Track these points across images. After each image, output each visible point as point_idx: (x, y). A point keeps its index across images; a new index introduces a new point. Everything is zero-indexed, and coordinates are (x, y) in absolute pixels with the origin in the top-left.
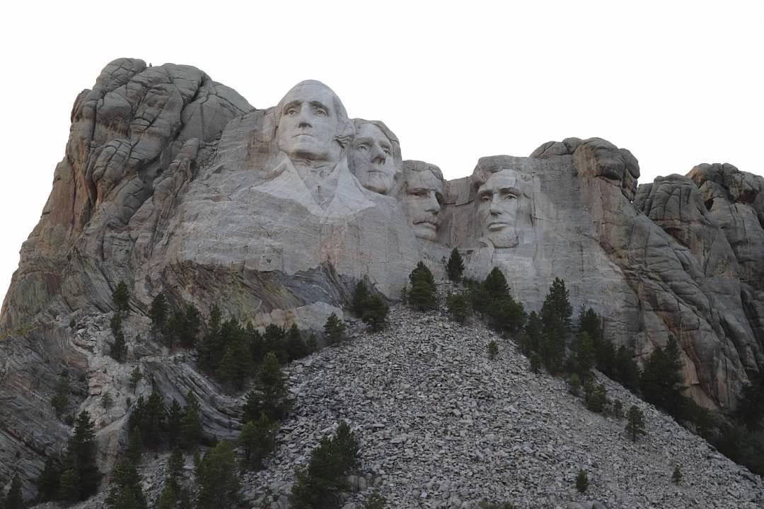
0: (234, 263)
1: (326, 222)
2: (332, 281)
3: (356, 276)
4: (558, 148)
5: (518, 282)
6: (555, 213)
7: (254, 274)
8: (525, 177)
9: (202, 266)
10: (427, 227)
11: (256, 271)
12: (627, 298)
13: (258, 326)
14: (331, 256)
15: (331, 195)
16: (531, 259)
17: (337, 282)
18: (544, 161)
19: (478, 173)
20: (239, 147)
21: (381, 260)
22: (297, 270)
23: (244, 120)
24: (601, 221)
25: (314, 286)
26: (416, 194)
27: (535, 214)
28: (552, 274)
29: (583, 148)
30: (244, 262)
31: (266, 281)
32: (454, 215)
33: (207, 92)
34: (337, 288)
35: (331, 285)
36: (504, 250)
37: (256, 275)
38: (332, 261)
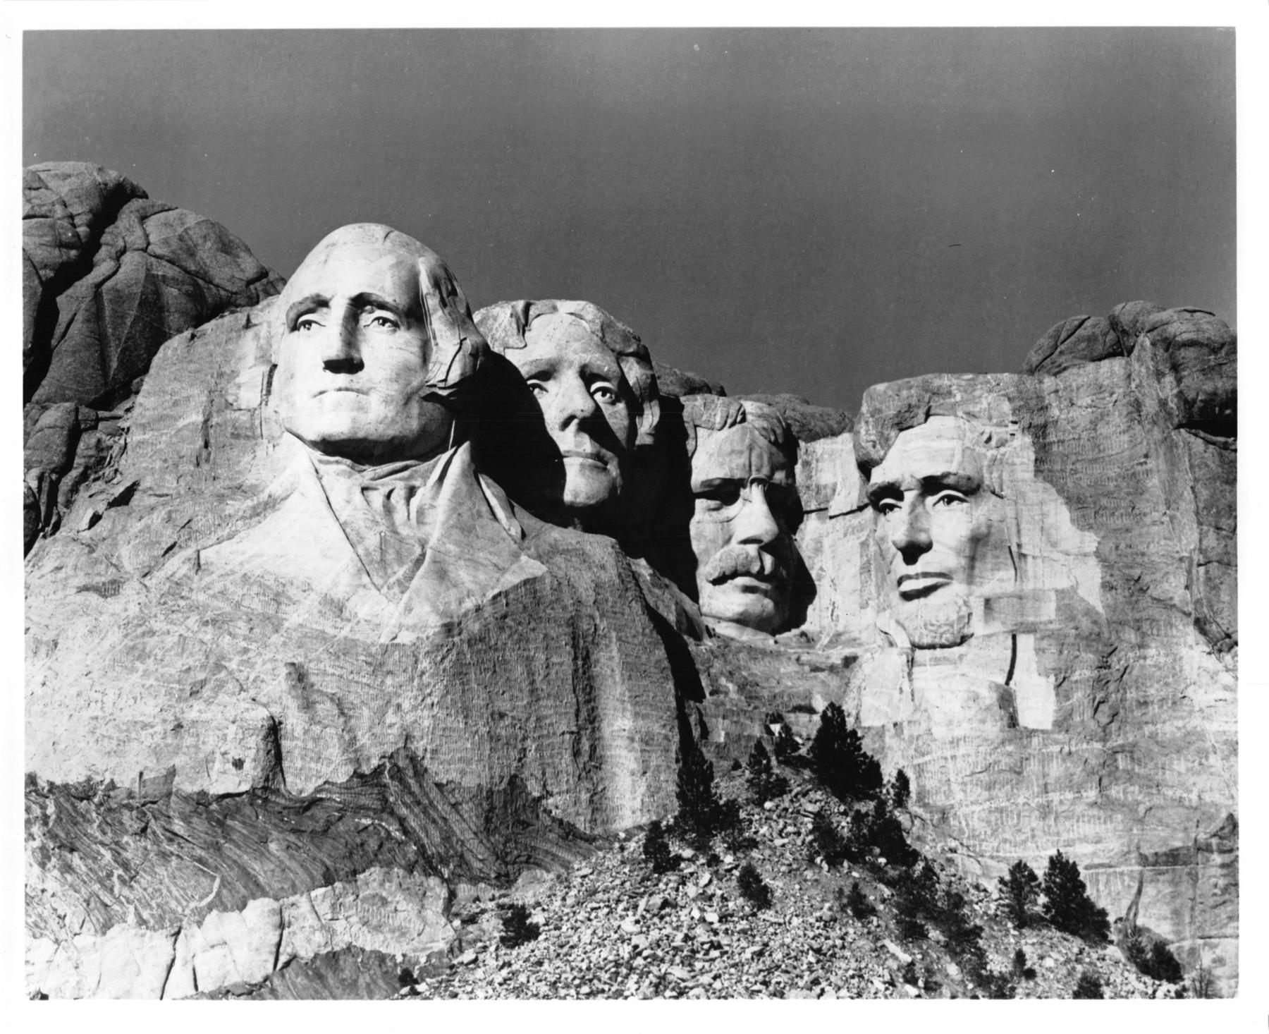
0: (145, 777)
2: (418, 803)
3: (483, 783)
7: (201, 801)
8: (989, 439)
11: (203, 794)
13: (213, 947)
14: (417, 734)
16: (1001, 680)
17: (431, 803)
18: (1049, 382)
20: (181, 423)
21: (564, 728)
22: (320, 782)
23: (198, 342)
24: (1197, 557)
25: (369, 822)
27: (1019, 546)
30: (172, 773)
31: (229, 822)
33: (121, 243)
34: (434, 821)
35: (416, 816)
36: (939, 652)
37: (207, 806)
38: (419, 746)
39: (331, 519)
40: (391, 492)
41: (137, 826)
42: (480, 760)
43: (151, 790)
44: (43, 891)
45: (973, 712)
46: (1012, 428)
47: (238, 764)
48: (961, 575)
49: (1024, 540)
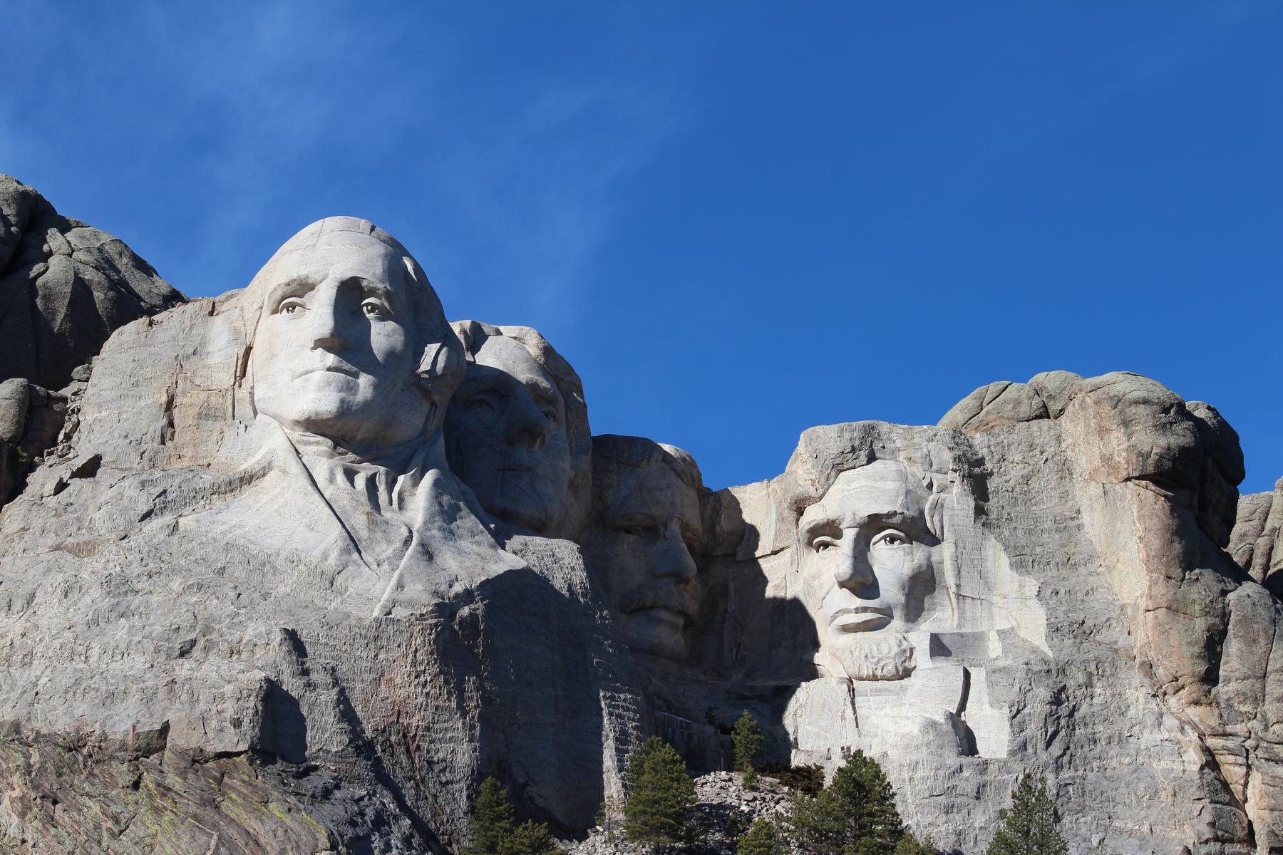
1: (390, 613)
4: (1017, 403)
5: (919, 774)
6: (1016, 584)
7: (197, 760)
8: (930, 486)
9: (50, 739)
10: (660, 621)
12: (1218, 816)
15: (405, 533)
19: (800, 472)
22: (314, 750)
26: (628, 532)
28: (1012, 753)
29: (1089, 401)
30: (165, 729)
32: (732, 587)
36: (879, 684)
39: (316, 496)
40: (374, 475)
41: (129, 779)
42: (471, 741)
43: (142, 743)
44: (24, 841)
45: (931, 738)
46: (951, 475)
47: (237, 723)
48: (898, 614)
49: (964, 581)
